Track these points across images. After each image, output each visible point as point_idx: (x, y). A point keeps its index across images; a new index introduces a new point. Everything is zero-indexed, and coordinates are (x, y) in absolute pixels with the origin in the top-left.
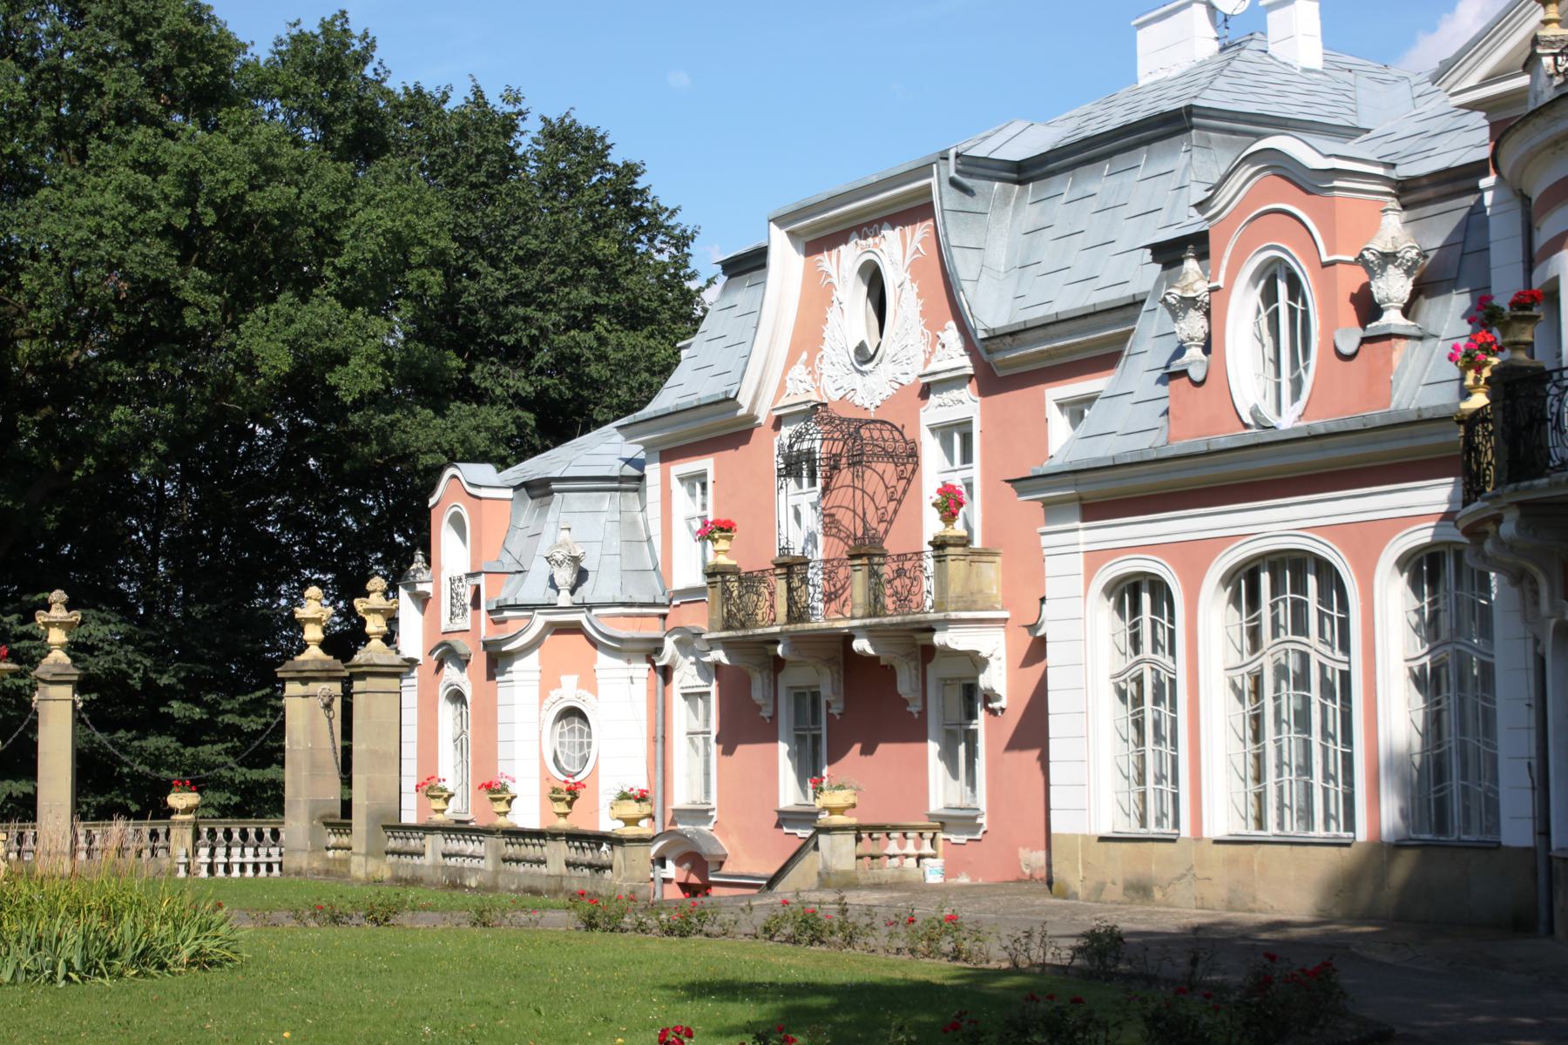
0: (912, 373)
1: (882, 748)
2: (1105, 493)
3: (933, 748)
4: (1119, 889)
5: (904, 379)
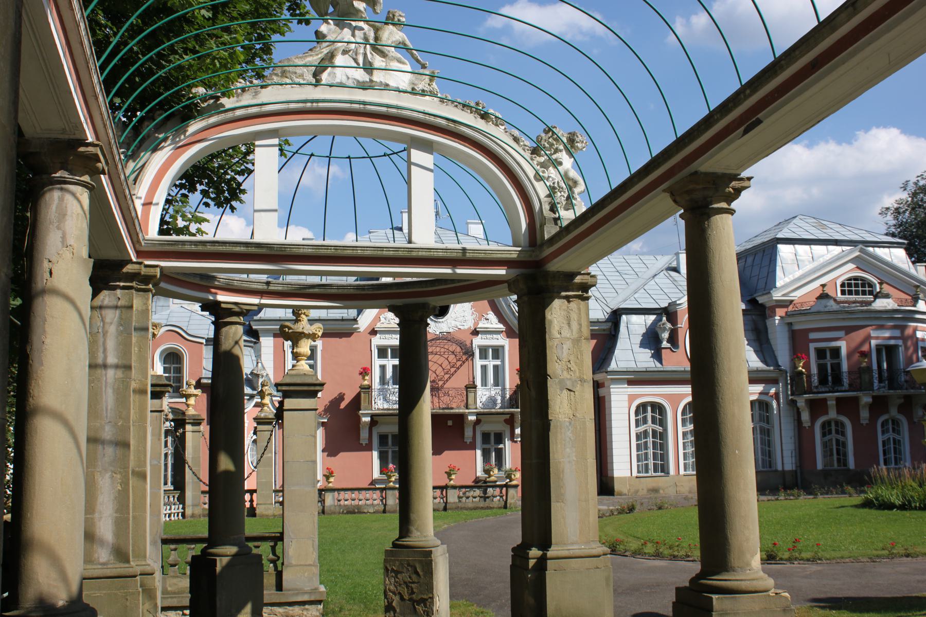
0: (469, 324)
1: (446, 452)
2: (638, 379)
3: (479, 453)
4: (645, 491)
5: (462, 328)
